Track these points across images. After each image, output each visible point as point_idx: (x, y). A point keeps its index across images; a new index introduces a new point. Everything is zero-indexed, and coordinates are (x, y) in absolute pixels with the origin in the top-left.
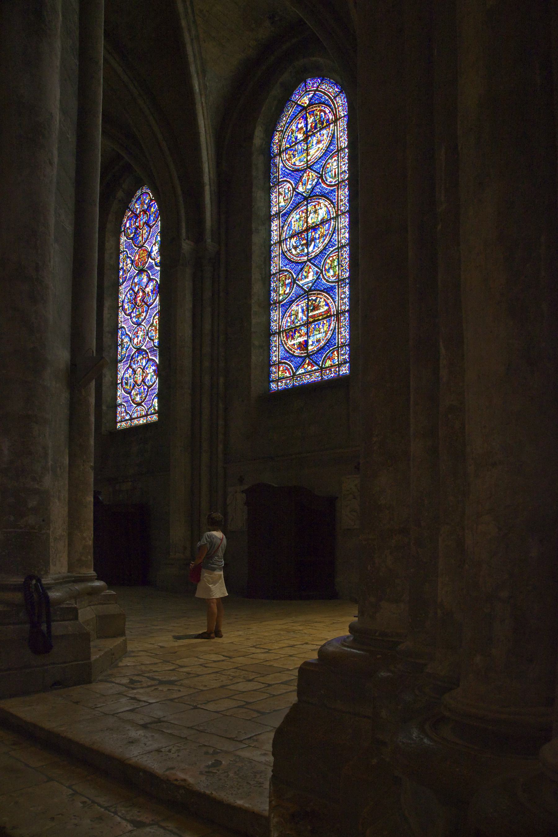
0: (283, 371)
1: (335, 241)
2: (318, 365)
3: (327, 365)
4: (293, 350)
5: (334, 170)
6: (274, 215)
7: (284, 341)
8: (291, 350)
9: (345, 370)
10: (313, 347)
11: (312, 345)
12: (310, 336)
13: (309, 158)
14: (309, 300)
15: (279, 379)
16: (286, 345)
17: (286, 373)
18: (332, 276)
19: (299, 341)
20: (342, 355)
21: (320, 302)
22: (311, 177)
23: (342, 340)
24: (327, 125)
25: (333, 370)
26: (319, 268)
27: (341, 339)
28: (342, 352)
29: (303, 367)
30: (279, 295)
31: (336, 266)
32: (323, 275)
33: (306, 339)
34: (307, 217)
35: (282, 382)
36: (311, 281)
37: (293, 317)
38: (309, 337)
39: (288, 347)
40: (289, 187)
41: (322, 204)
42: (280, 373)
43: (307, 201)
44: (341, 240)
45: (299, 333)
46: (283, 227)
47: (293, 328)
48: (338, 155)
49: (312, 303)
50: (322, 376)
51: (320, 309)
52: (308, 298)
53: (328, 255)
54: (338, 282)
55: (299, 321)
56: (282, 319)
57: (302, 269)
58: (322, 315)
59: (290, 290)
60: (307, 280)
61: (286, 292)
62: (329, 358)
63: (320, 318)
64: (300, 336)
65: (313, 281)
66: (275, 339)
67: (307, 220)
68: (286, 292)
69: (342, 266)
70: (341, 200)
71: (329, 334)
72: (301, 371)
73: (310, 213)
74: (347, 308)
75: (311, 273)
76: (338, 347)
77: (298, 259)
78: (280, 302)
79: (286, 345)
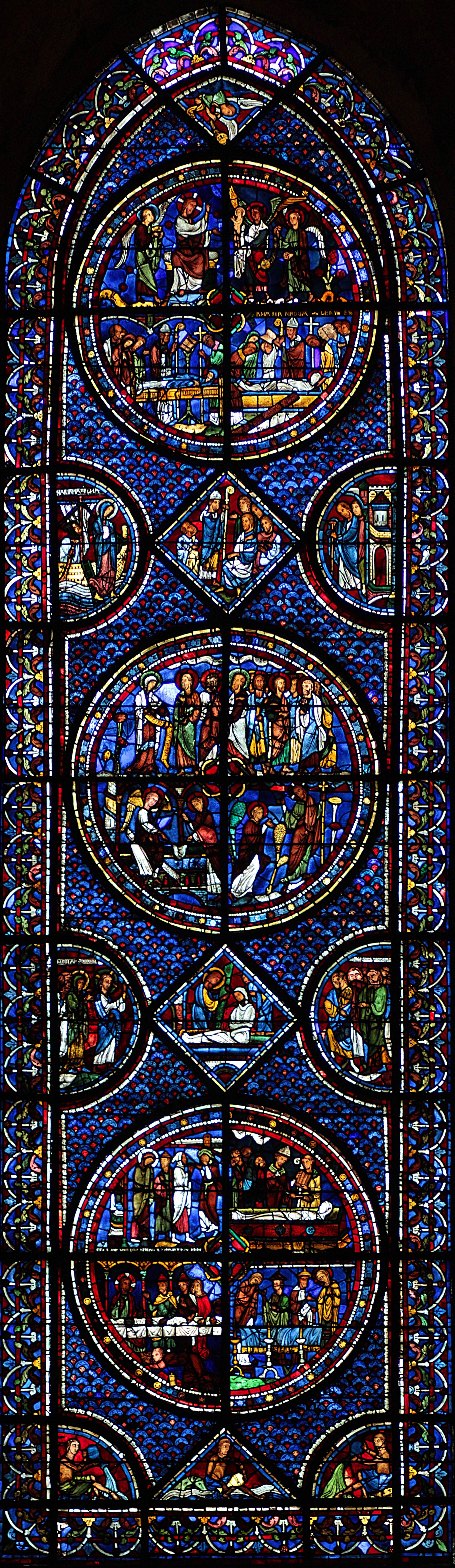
0: (83, 1465)
1: (379, 894)
2: (289, 1480)
3: (332, 1489)
4: (141, 1369)
5: (373, 548)
6: (21, 623)
7: (88, 1309)
8: (132, 1370)
9: (431, 1536)
10: (253, 1383)
11: (249, 1372)
12: (240, 1325)
13: (236, 418)
14: (230, 1143)
15: (53, 1503)
16: (101, 1335)
17: (102, 1480)
18: (359, 1060)
19: (181, 1332)
20: (420, 1460)
21: (292, 1170)
22: (247, 521)
23: (416, 1391)
24: (337, 306)
25: (365, 1520)
26: (290, 1002)
27: (409, 1383)
28: (416, 1447)
29: (199, 1471)
30: (61, 1063)
31: (381, 1020)
32: (309, 1043)
33: (218, 1331)
34: (227, 720)
35: (76, 1523)
36: (243, 1051)
37: (136, 1204)
38: (233, 1327)
39: (110, 1348)
40: (119, 520)
41: (307, 685)
42: (66, 1472)
43: (226, 640)
44: (407, 905)
45: (177, 1291)
46: (78, 711)
47: (138, 1256)
48: (398, 477)
49: (248, 1162)
50: (304, 1534)
51: (292, 1206)
52: (227, 1130)
53: (339, 951)
54: (392, 1101)
55: (174, 1229)
56: (76, 1193)
57: (190, 970)
58: (308, 1240)
59: (120, 1053)
60: (220, 1037)
61: (99, 1059)
62: (345, 1457)
63: (298, 1249)
64: (186, 1310)
65: (258, 1053)
66: (33, 1285)
67: (224, 732)
68: (99, 1059)
69: (412, 1032)
70: (413, 712)
71: (344, 1347)
72: (186, 1488)
73: (242, 706)
74: (440, 1239)
75: (246, 1013)
76: (393, 1415)
77: (172, 909)
78: (61, 1100)
79: (101, 1335)
